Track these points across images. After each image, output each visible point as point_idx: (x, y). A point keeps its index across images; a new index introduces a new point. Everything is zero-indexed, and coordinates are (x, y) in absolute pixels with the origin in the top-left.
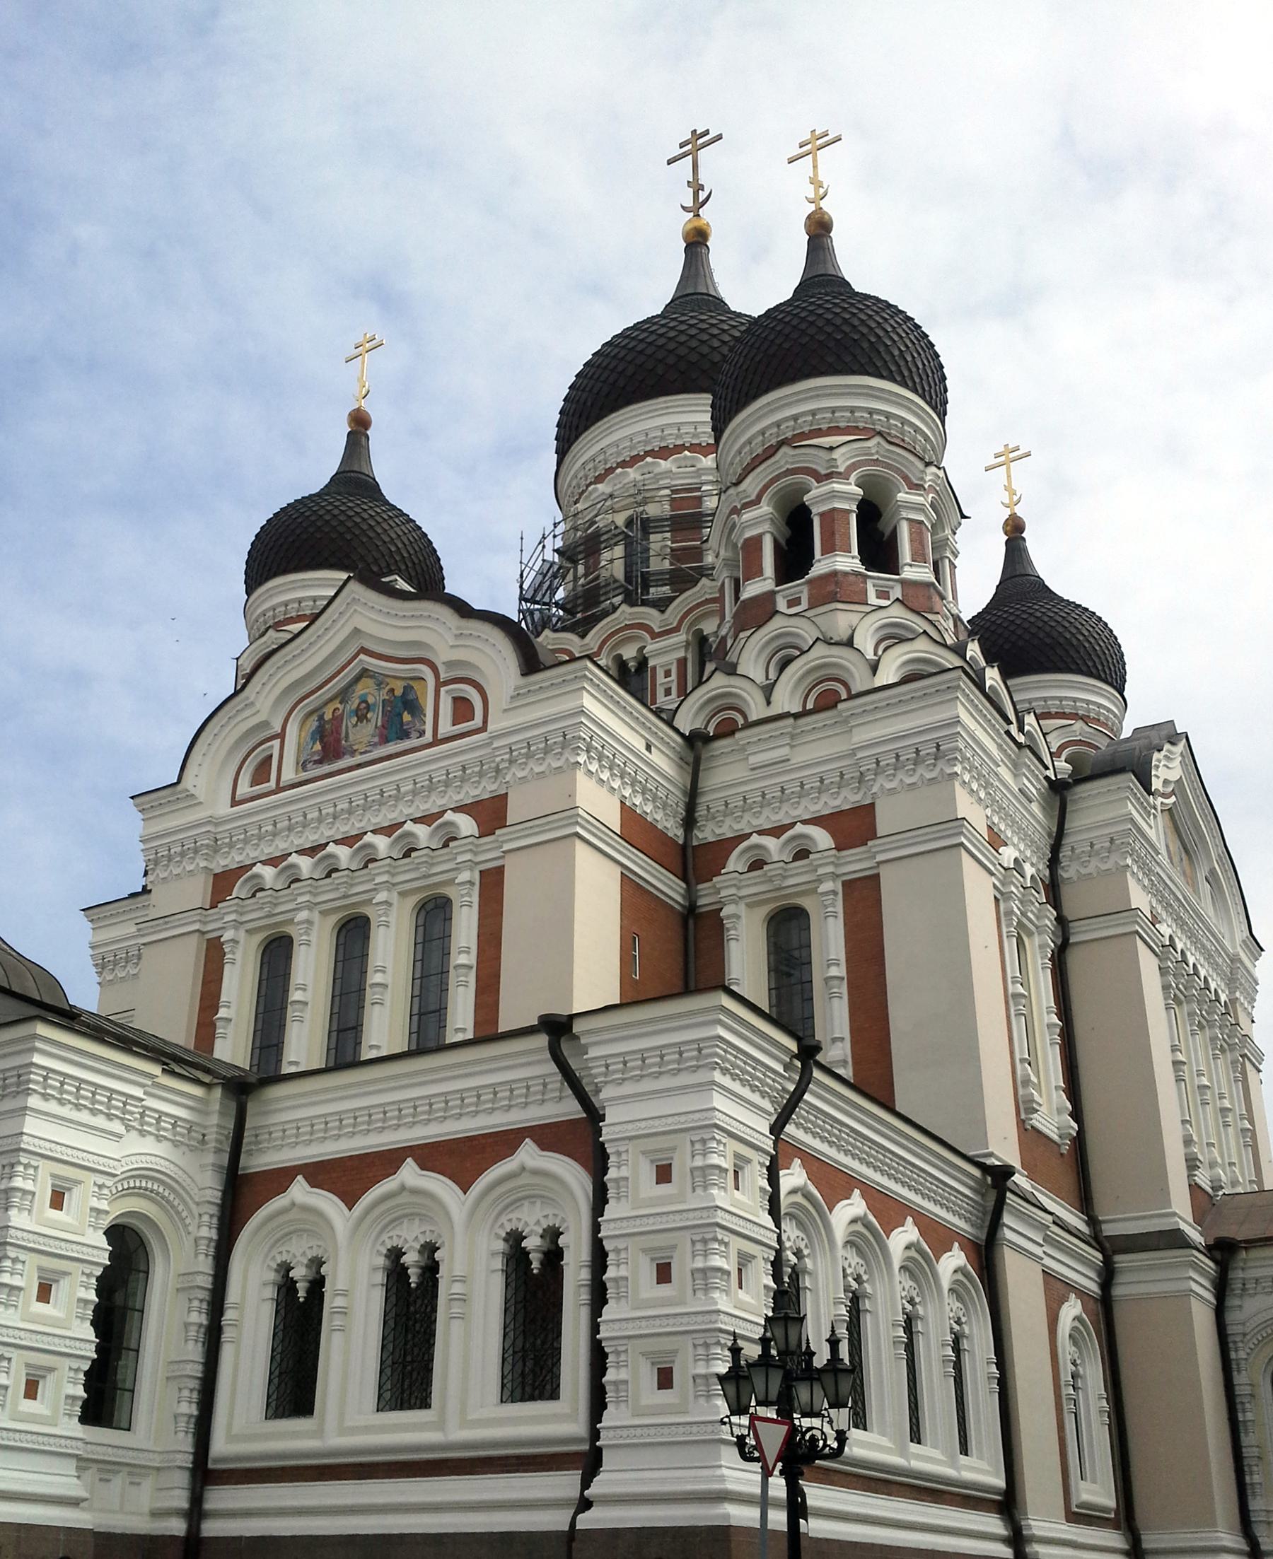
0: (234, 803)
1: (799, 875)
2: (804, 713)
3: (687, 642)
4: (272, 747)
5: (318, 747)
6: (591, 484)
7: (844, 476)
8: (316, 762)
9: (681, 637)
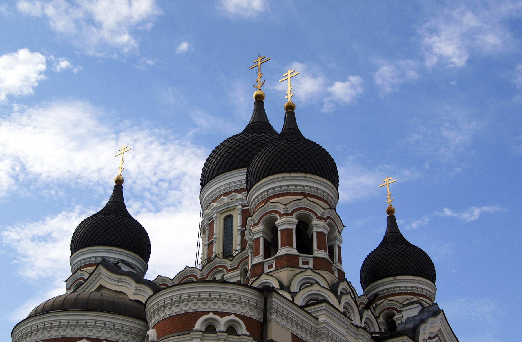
3: (241, 273)
6: (211, 203)
7: (291, 214)
9: (238, 272)
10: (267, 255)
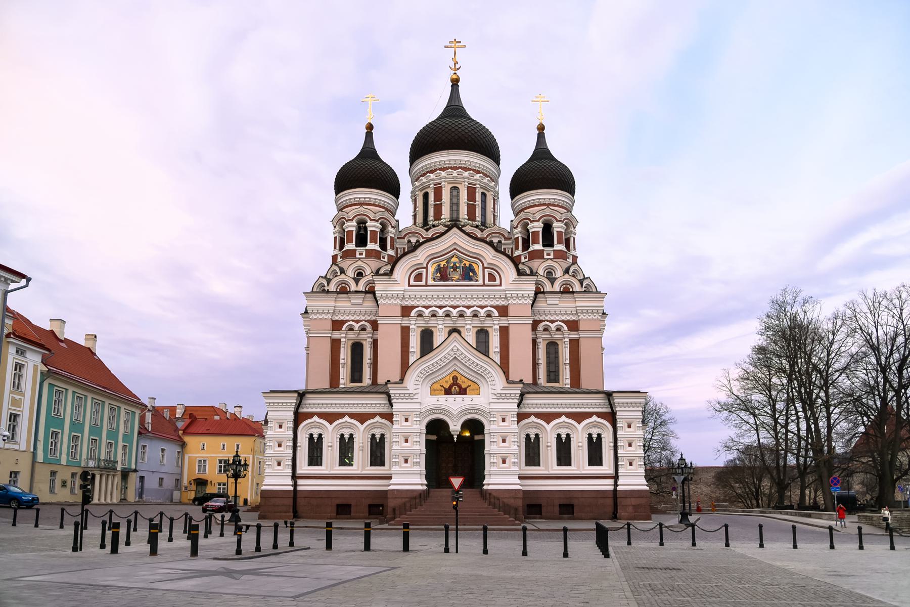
0: (409, 285)
1: (558, 335)
2: (560, 292)
4: (423, 271)
5: (438, 275)
6: (436, 170)
8: (438, 279)
10: (544, 246)
